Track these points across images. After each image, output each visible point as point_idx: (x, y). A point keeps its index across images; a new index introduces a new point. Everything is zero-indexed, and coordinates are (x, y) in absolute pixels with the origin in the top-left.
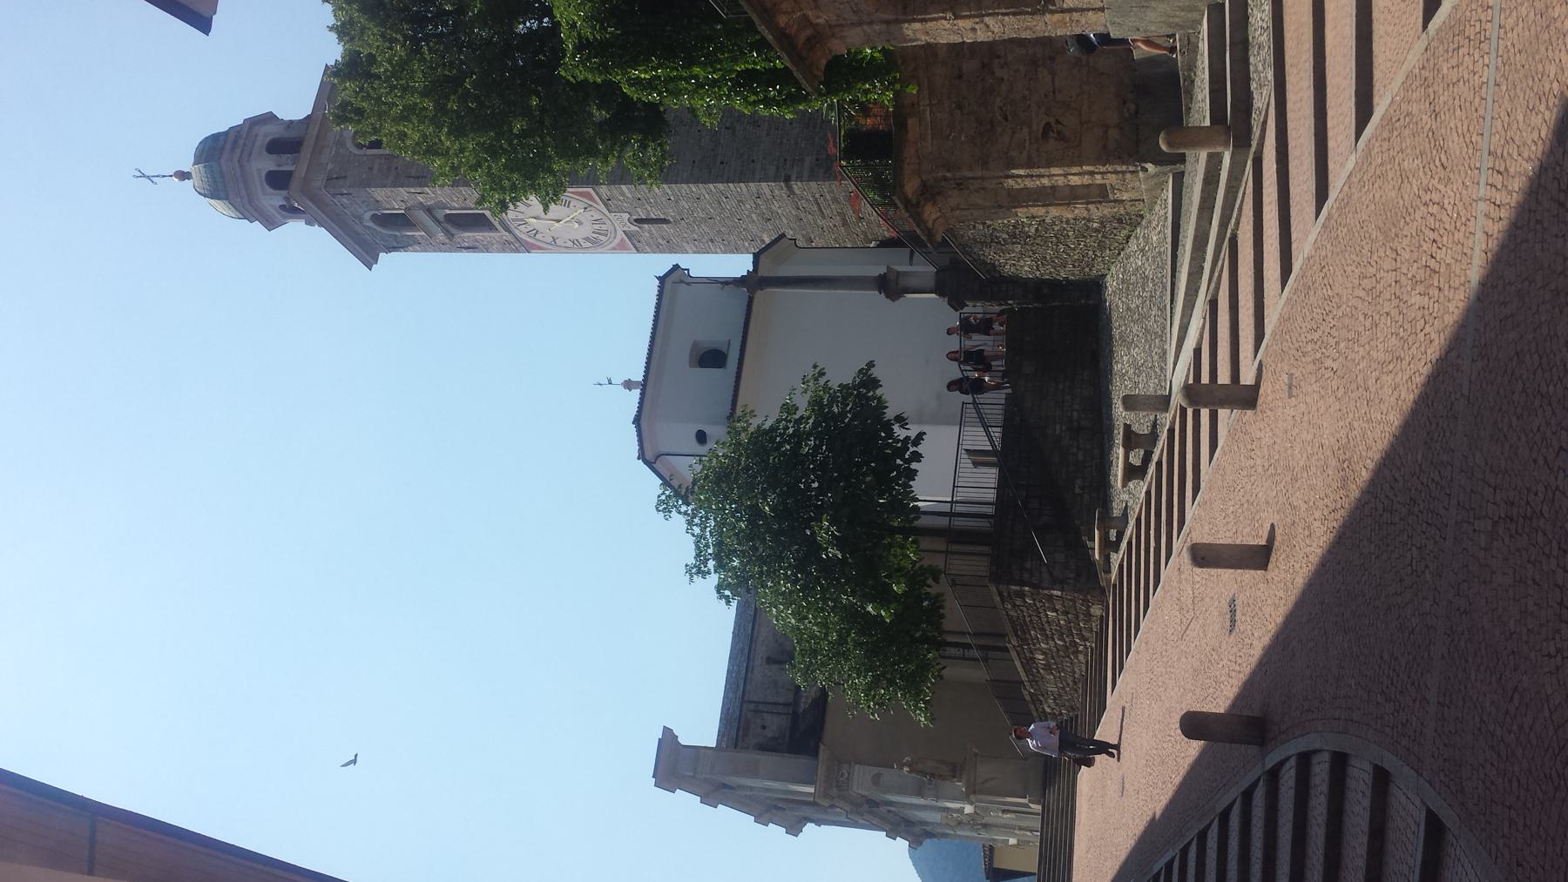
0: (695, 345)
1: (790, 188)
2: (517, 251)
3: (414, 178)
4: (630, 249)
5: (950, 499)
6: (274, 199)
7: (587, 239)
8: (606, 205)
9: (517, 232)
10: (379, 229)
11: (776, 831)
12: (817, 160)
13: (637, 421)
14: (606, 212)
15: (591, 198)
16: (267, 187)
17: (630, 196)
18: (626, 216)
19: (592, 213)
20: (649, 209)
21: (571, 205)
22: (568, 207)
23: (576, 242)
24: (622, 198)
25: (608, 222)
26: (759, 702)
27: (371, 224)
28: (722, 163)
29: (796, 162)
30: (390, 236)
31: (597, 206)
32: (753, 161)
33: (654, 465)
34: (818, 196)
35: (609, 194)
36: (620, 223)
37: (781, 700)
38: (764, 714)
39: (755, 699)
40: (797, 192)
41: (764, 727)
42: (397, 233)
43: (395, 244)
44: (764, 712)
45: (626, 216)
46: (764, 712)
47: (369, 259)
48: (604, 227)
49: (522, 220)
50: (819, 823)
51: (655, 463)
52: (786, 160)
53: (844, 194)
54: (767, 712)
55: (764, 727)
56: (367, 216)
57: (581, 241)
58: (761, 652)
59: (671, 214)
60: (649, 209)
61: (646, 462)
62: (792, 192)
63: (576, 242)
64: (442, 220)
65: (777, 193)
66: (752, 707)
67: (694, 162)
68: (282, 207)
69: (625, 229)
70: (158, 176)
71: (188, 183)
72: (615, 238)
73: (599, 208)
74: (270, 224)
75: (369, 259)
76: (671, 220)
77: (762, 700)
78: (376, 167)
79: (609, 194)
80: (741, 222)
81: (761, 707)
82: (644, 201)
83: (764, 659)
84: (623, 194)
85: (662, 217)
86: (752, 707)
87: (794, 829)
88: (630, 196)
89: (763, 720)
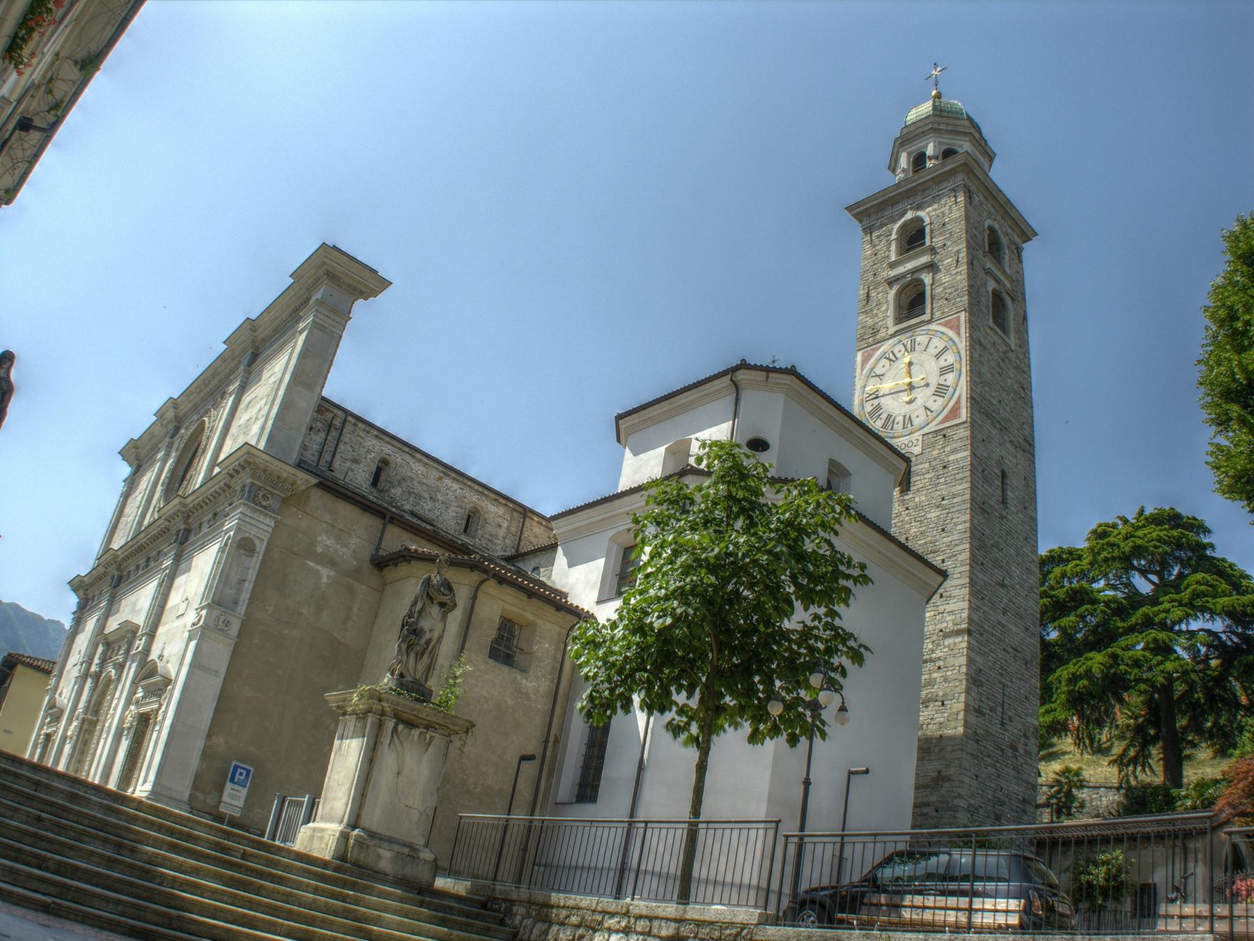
1: (958, 633)
16: (945, 147)
21: (937, 398)
22: (934, 394)
24: (948, 449)
26: (342, 430)
31: (940, 418)
32: (982, 599)
34: (941, 663)
35: (955, 437)
37: (337, 463)
38: (324, 436)
39: (345, 430)
40: (948, 641)
42: (894, 236)
44: (327, 435)
46: (327, 435)
52: (981, 634)
53: (941, 693)
54: (326, 439)
58: (397, 458)
62: (947, 635)
64: (915, 276)
65: (949, 618)
66: (337, 423)
67: (983, 534)
77: (342, 437)
79: (955, 437)
81: (334, 434)
83: (388, 457)
84: (954, 451)
86: (337, 423)
88: (952, 458)
89: (319, 430)
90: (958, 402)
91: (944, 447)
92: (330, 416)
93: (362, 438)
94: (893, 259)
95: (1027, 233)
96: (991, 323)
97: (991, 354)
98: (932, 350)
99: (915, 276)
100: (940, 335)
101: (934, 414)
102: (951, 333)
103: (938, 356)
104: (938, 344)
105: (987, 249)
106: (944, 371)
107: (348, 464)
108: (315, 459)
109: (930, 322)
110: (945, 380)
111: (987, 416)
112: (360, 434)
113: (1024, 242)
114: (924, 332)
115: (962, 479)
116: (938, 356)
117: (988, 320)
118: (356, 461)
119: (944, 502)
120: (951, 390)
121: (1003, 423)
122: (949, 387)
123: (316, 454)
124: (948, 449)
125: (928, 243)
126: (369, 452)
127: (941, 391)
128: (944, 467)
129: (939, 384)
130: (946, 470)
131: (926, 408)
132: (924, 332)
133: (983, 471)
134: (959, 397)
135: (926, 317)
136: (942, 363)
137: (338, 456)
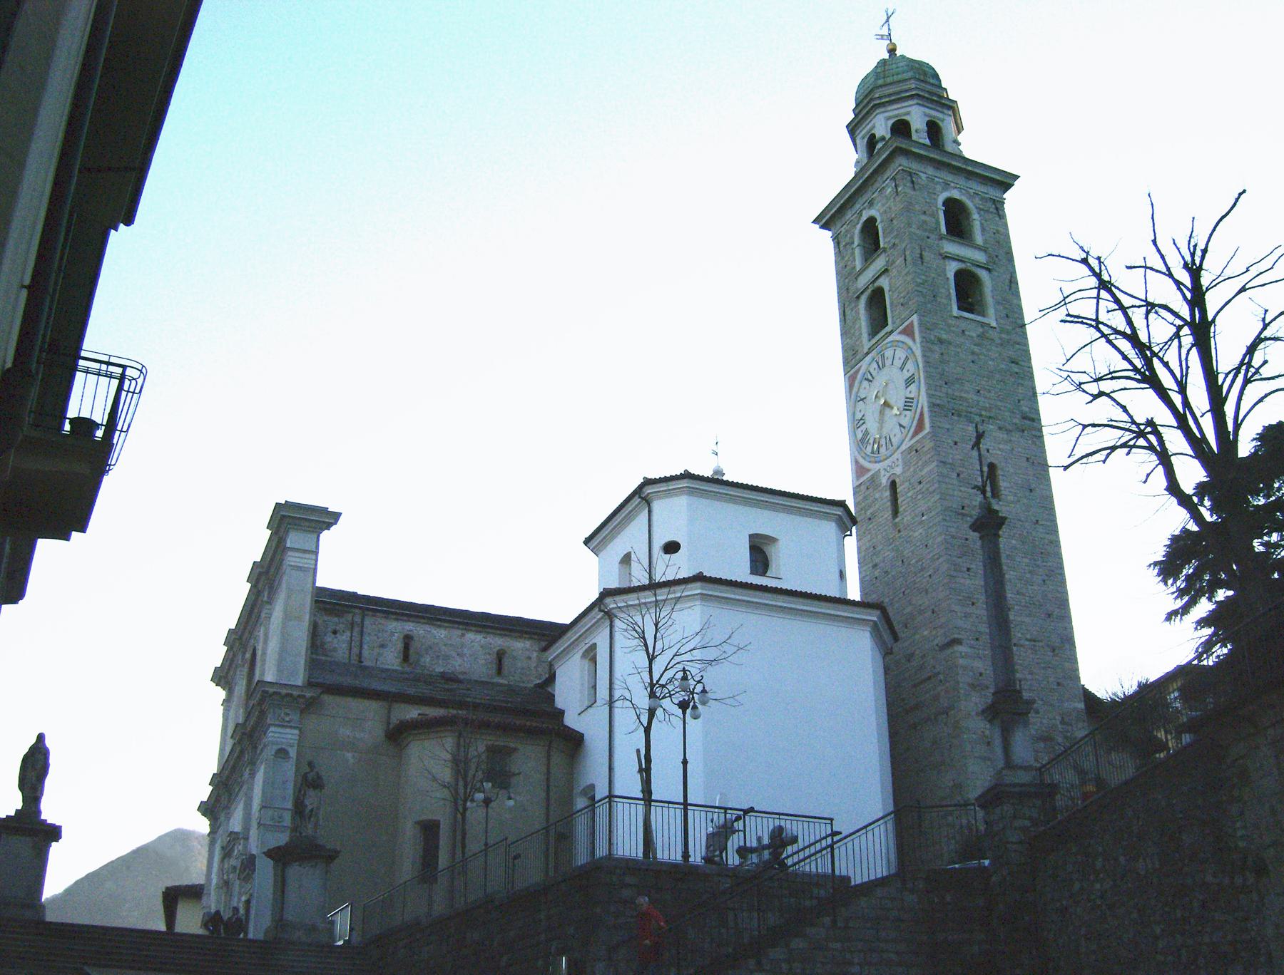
0: (772, 540)
2: (846, 361)
3: (921, 254)
4: (858, 479)
5: (679, 813)
6: (881, 126)
7: (866, 433)
8: (910, 448)
9: (868, 359)
10: (859, 226)
11: (217, 653)
12: (981, 674)
13: (687, 475)
14: (904, 447)
15: (916, 433)
17: (923, 473)
18: (898, 470)
19: (899, 435)
20: (909, 494)
23: (862, 422)
24: (920, 463)
25: (888, 453)
26: (362, 627)
27: (864, 218)
28: (968, 570)
29: (977, 652)
30: (852, 238)
32: (973, 604)
33: (637, 496)
35: (925, 449)
36: (890, 467)
37: (366, 653)
38: (348, 634)
41: (335, 632)
42: (857, 241)
43: (841, 246)
45: (898, 470)
47: (827, 220)
48: (883, 450)
49: (884, 365)
50: (226, 703)
51: (640, 497)
52: (977, 639)
55: (335, 632)
56: (873, 213)
57: (863, 428)
59: (905, 517)
60: (909, 494)
61: (641, 487)
63: (862, 422)
64: (876, 284)
67: (967, 539)
68: (873, 136)
69: (883, 472)
70: (889, 29)
71: (886, 56)
72: (870, 462)
73: (905, 442)
74: (853, 129)
75: (827, 220)
76: (897, 520)
78: (923, 217)
79: (925, 449)
80: (901, 595)
82: (918, 489)
83: (410, 633)
84: (924, 466)
85: (901, 510)
86: (358, 619)
87: (222, 677)
89: (343, 631)
90: (922, 414)
91: (917, 463)
92: (349, 617)
93: (383, 624)
94: (858, 268)
95: (1004, 181)
96: (955, 311)
97: (959, 346)
98: (898, 363)
99: (876, 284)
100: (900, 344)
101: (907, 430)
102: (909, 342)
103: (902, 369)
104: (901, 354)
105: (943, 230)
106: (909, 381)
107: (377, 650)
108: (347, 656)
109: (891, 332)
110: (910, 392)
111: (959, 416)
112: (381, 621)
113: (1004, 193)
114: (889, 345)
115: (934, 491)
116: (902, 369)
117: (951, 311)
118: (382, 646)
119: (923, 518)
120: (915, 401)
121: (983, 413)
122: (913, 399)
123: (347, 652)
124: (920, 463)
125: (882, 246)
126: (392, 634)
127: (908, 404)
128: (920, 483)
129: (907, 398)
130: (922, 486)
131: (900, 425)
132: (889, 345)
133: (958, 475)
134: (922, 408)
135: (888, 329)
136: (906, 375)
137: (365, 647)
